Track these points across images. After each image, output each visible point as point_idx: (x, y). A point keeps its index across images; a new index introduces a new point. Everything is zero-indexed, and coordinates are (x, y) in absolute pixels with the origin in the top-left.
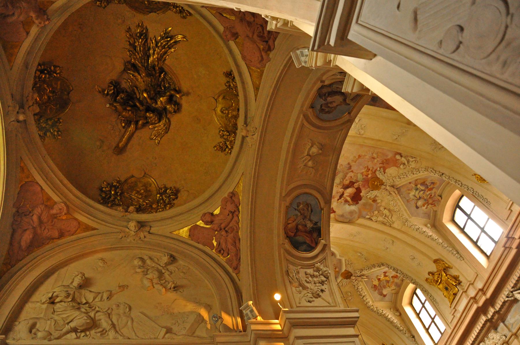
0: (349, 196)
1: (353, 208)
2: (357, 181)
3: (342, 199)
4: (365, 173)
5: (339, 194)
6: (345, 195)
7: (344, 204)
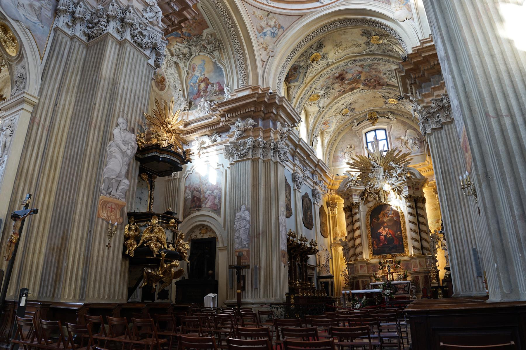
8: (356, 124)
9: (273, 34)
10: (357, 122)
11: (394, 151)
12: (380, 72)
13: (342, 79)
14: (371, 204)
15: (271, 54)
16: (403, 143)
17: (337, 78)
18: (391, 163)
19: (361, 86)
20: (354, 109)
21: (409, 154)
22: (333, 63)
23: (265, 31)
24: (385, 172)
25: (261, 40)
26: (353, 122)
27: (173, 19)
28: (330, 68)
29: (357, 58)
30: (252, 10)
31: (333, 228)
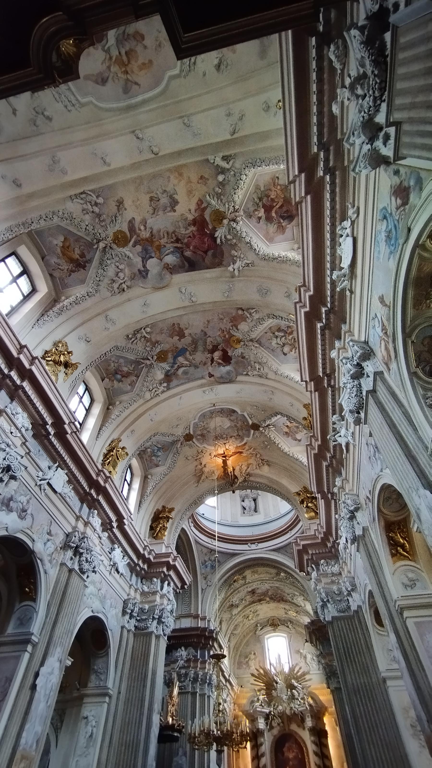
0: (219, 359)
1: (228, 368)
2: (219, 344)
3: (215, 362)
4: (222, 335)
5: (209, 360)
6: (215, 358)
7: (218, 367)
8: (260, 628)
9: (213, 567)
10: (260, 626)
11: (295, 667)
12: (284, 592)
13: (254, 593)
14: (275, 731)
15: (209, 584)
16: (302, 657)
17: (250, 592)
18: (293, 681)
19: (268, 599)
20: (259, 615)
21: (308, 673)
22: (249, 583)
23: (207, 564)
24: (287, 691)
25: (203, 571)
26: (257, 626)
27: (155, 571)
28: (246, 586)
29: (268, 582)
30: (200, 548)
31: (236, 760)
